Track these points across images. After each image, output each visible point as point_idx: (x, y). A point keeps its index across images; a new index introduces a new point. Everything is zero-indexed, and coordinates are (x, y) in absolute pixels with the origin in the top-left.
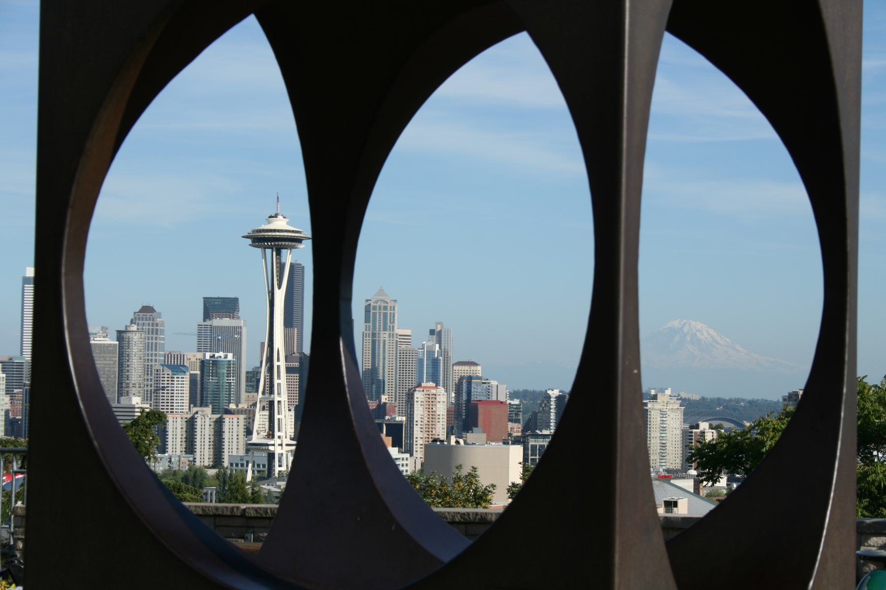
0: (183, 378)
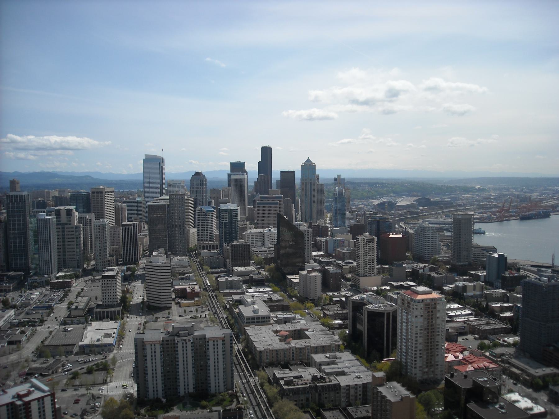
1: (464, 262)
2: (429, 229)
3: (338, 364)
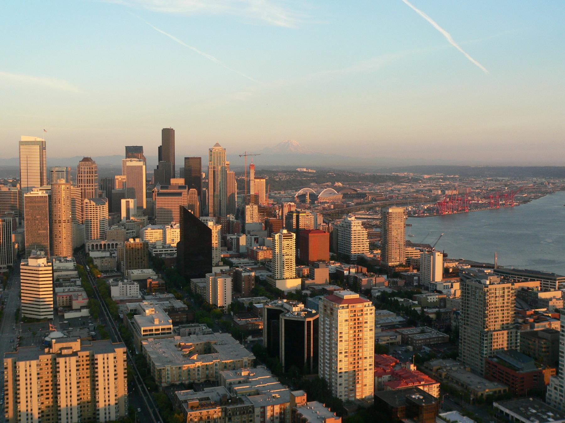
0: (103, 207)
1: (396, 262)
2: (356, 224)
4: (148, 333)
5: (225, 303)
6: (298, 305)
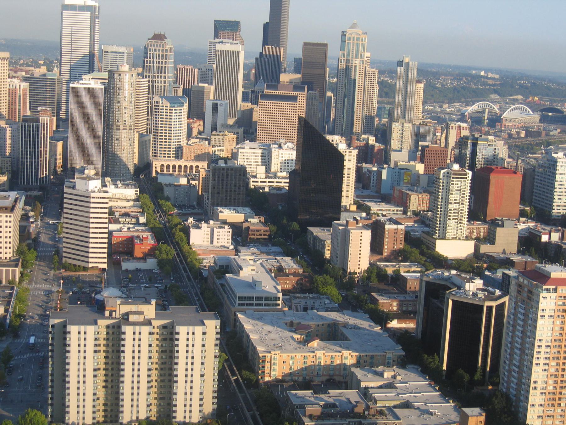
0: (181, 110)
3: (396, 388)
4: (246, 302)
5: (359, 268)
6: (474, 281)
